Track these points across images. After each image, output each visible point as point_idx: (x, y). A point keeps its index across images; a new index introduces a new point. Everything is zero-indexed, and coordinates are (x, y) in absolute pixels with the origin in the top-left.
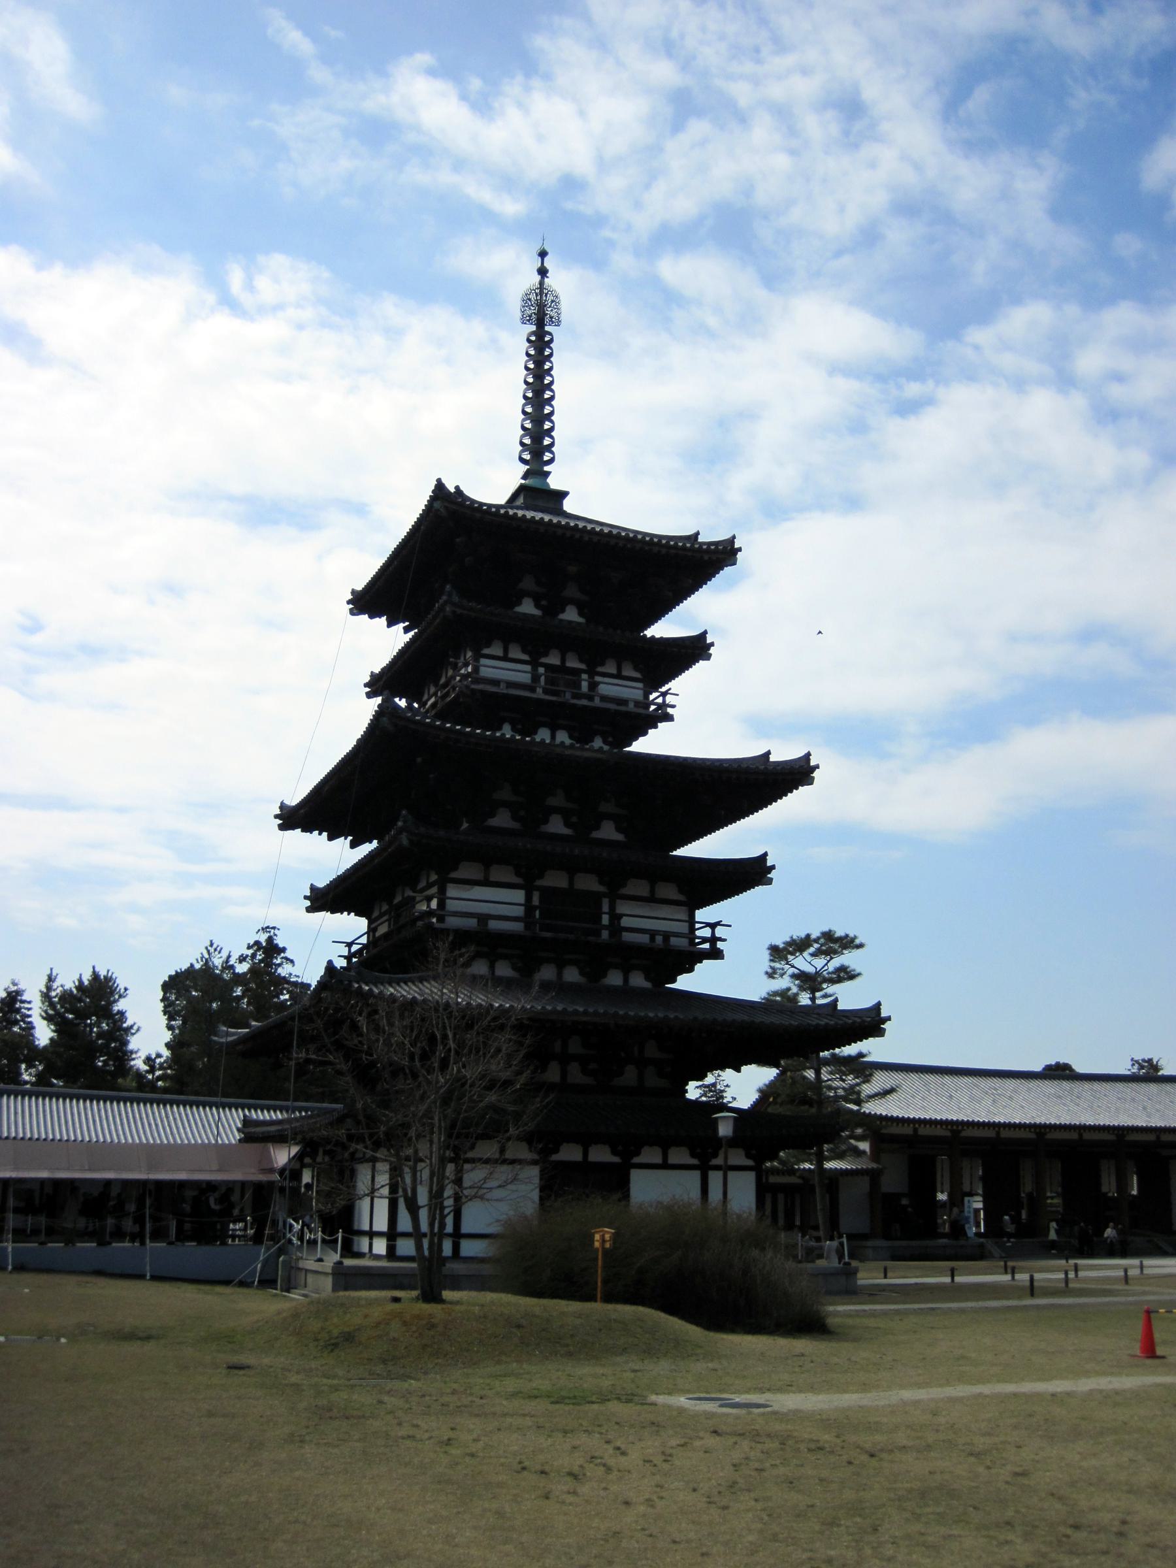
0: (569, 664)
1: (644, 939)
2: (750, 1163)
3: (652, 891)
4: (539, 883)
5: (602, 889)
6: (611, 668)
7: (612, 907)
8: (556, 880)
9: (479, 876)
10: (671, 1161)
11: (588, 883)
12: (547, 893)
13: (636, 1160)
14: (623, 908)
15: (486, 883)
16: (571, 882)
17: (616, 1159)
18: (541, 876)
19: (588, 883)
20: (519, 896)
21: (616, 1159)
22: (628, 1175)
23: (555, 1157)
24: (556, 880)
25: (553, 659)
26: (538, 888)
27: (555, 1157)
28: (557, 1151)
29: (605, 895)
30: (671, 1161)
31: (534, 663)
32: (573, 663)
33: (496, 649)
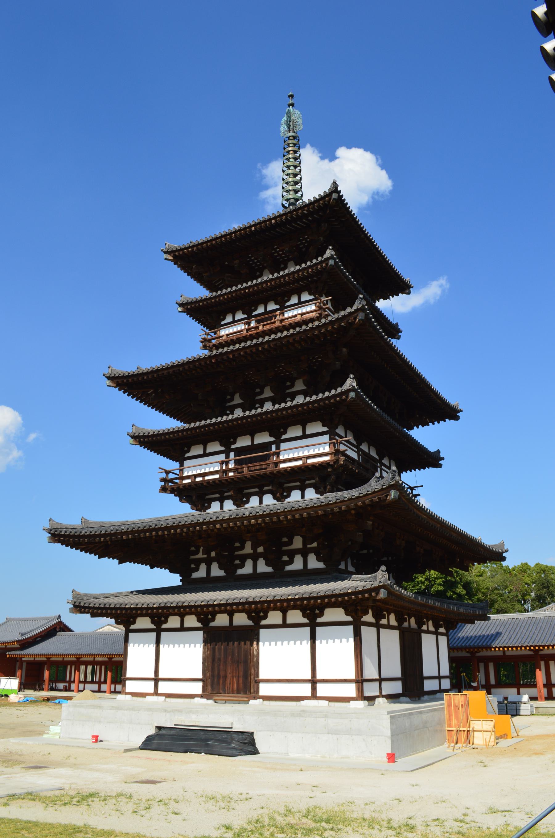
0: (269, 309)
1: (300, 463)
2: (350, 619)
3: (304, 431)
4: (233, 446)
5: (273, 439)
6: (294, 300)
7: (278, 447)
8: (243, 442)
9: (201, 452)
10: (289, 621)
11: (263, 438)
12: (239, 451)
13: (264, 622)
14: (283, 446)
15: (205, 455)
16: (252, 441)
17: (250, 623)
18: (235, 442)
19: (263, 438)
20: (222, 457)
21: (250, 623)
22: (258, 635)
23: (212, 624)
24: (243, 442)
25: (261, 310)
26: (234, 450)
27: (212, 624)
28: (213, 619)
29: (271, 443)
30: (289, 621)
31: (250, 317)
32: (272, 306)
33: (229, 319)
